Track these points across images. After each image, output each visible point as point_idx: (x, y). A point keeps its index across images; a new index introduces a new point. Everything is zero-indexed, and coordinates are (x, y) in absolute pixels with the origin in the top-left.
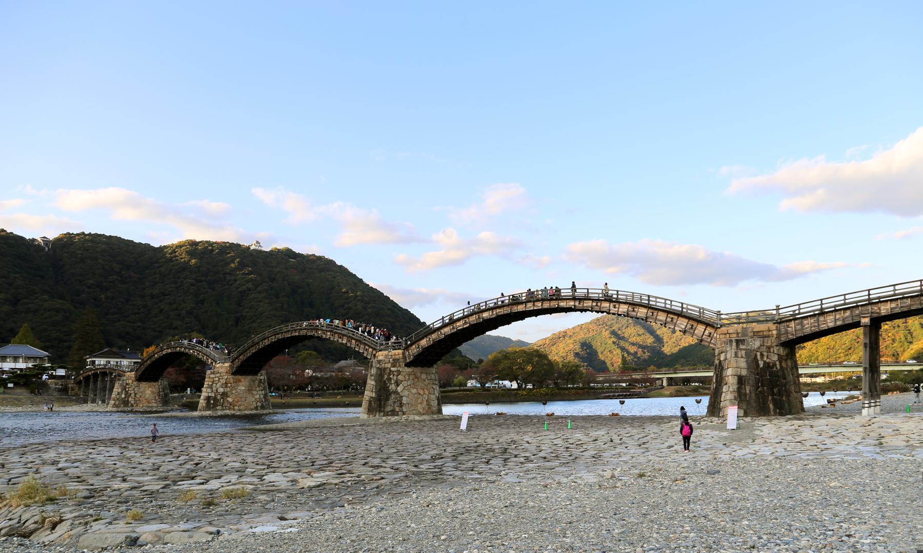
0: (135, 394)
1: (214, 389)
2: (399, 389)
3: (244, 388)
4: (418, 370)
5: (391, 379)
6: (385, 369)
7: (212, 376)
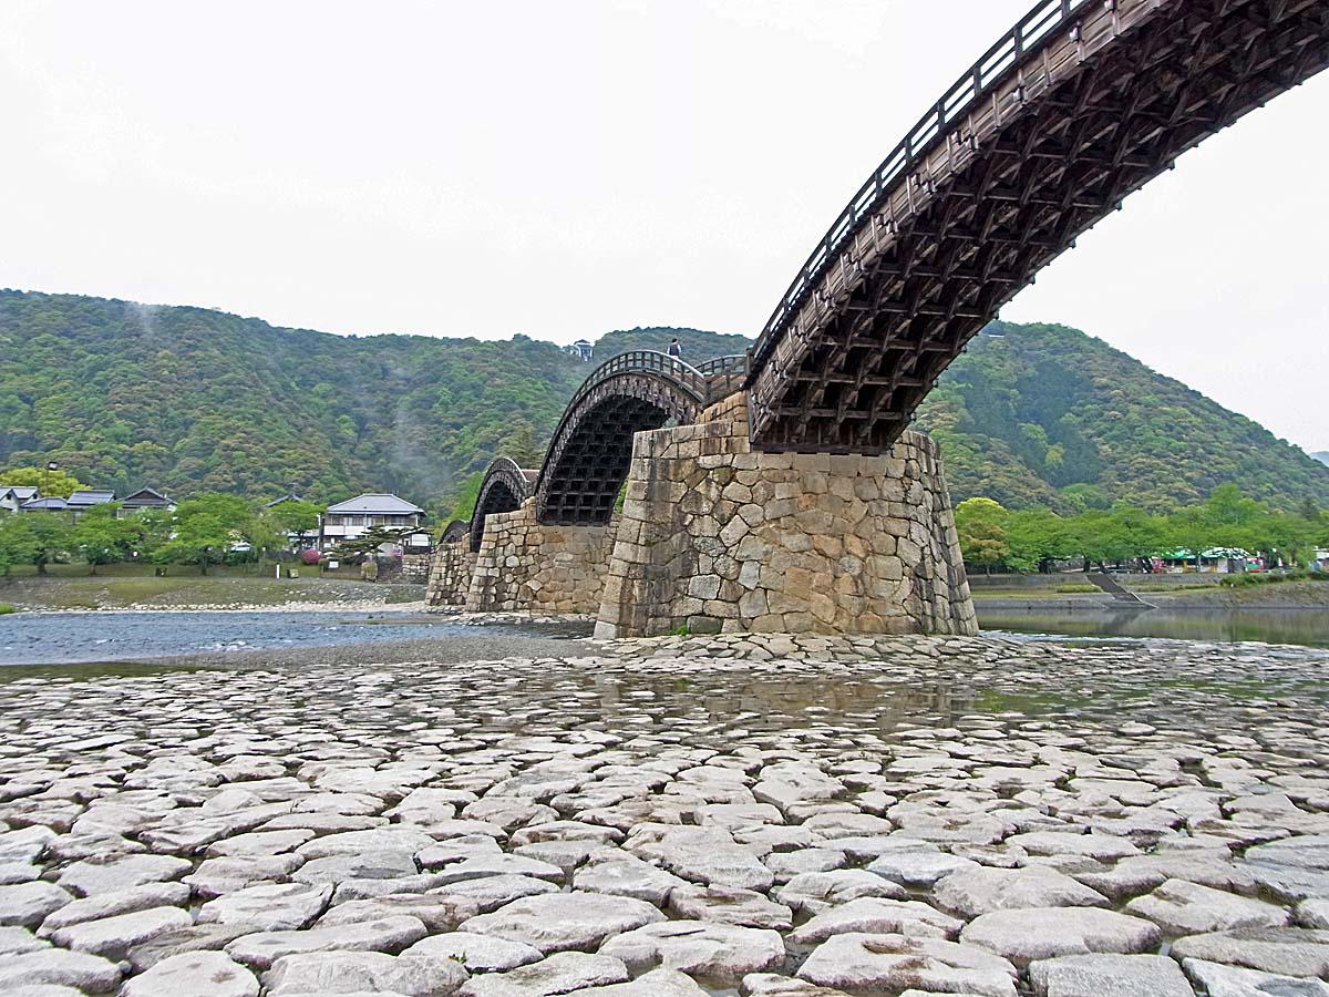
1: (500, 559)
3: (571, 557)
5: (697, 498)
6: (679, 460)
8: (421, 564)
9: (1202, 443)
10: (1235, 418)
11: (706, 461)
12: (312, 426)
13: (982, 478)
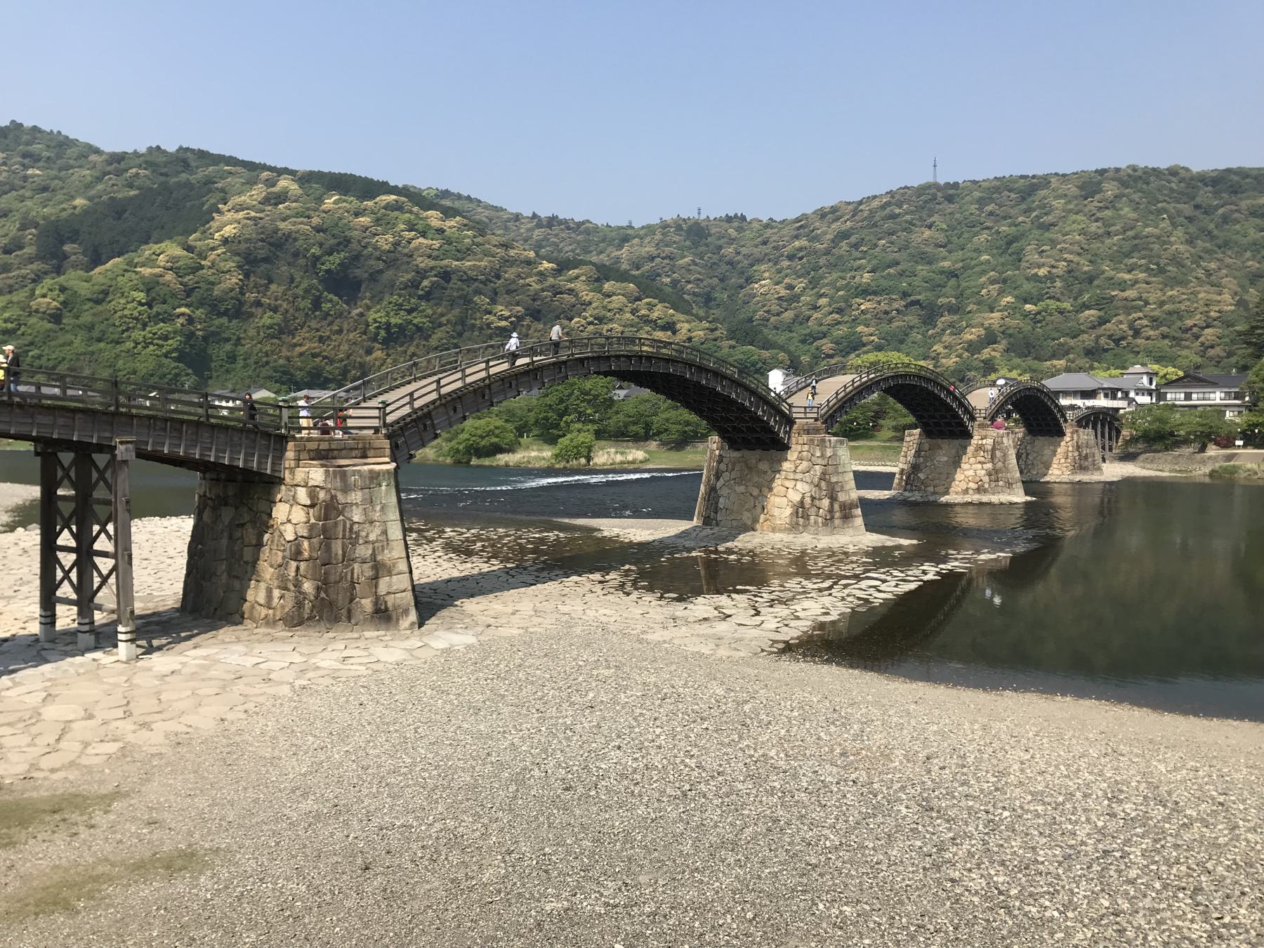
0: (1028, 454)
3: (946, 459)
4: (752, 456)
12: (1228, 266)
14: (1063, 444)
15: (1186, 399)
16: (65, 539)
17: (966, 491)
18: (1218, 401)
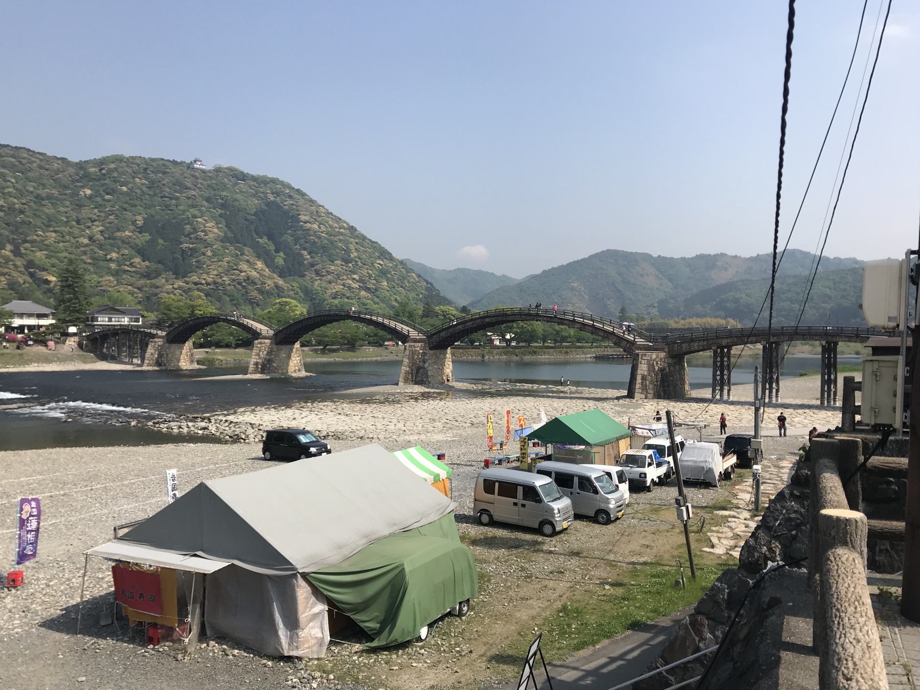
0: (167, 354)
2: (426, 366)
4: (438, 351)
7: (259, 346)
8: (74, 342)
9: (360, 259)
10: (375, 245)
11: (421, 351)
13: (241, 272)
14: (185, 348)
15: (108, 322)
16: (718, 373)
17: (295, 371)
18: (126, 323)
